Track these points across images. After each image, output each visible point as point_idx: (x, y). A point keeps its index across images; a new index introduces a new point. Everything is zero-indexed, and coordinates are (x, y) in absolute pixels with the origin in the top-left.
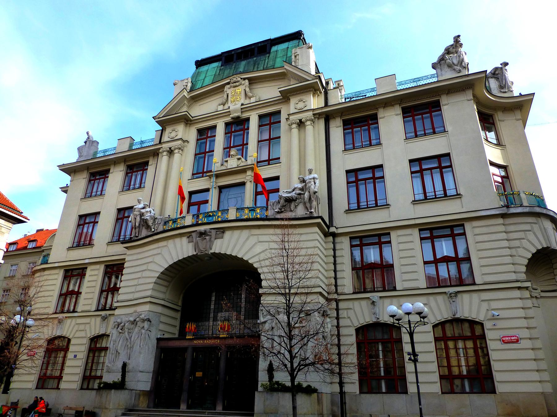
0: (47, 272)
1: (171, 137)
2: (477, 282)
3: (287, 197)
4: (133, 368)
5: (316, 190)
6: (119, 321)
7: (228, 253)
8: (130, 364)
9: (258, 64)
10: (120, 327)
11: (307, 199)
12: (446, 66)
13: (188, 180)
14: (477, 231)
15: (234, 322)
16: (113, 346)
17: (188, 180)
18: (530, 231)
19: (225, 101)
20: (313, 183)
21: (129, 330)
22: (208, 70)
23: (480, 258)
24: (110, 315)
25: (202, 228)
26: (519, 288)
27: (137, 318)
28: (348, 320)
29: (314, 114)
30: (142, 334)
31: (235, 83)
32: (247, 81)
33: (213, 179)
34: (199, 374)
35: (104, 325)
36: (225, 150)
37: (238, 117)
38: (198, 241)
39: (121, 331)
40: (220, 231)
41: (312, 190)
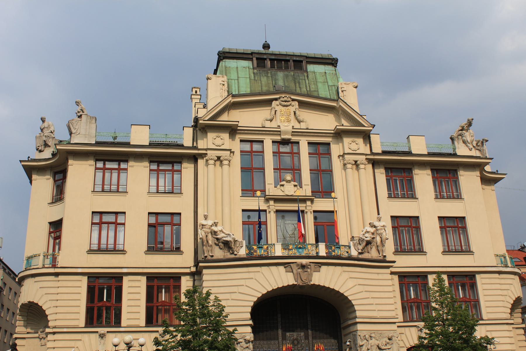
0: (61, 277)
1: (216, 145)
2: (484, 318)
5: (387, 237)
9: (299, 83)
12: (461, 141)
14: (484, 281)
15: (303, 341)
18: (512, 284)
19: (273, 117)
20: (384, 230)
22: (237, 68)
23: (486, 301)
25: (304, 261)
26: (507, 324)
27: (240, 339)
28: (402, 341)
29: (366, 159)
31: (285, 102)
32: (297, 103)
37: (289, 139)
40: (318, 265)
41: (384, 237)
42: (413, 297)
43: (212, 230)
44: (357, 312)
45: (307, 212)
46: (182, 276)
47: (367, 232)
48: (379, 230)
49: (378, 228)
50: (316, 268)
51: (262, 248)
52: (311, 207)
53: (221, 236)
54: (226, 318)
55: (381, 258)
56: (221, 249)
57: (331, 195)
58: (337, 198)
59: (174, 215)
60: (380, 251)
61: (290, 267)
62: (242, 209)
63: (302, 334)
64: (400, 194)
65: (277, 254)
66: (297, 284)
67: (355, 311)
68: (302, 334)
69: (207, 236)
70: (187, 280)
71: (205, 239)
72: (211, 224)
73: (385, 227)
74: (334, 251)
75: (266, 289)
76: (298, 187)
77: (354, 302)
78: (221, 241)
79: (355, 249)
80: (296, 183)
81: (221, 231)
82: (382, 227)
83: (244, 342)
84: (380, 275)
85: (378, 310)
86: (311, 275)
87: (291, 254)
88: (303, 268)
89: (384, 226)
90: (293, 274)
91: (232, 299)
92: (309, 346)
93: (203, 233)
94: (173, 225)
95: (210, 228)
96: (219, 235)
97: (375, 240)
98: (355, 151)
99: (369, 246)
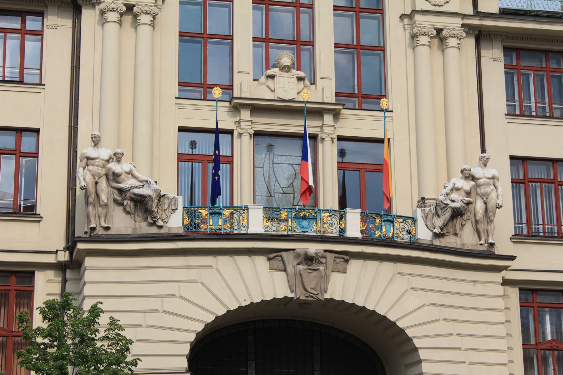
5: (500, 202)
20: (492, 187)
25: (312, 248)
29: (463, 25)
38: (303, 273)
40: (343, 258)
41: (493, 201)
42: (549, 337)
43: (109, 170)
44: (424, 364)
45: (323, 139)
46: (38, 271)
47: (456, 189)
48: (481, 185)
49: (481, 181)
50: (337, 264)
51: (220, 214)
52: (333, 128)
53: (130, 184)
54: (133, 368)
55: (484, 248)
56: (128, 213)
57: (379, 103)
58: (392, 111)
59: (23, 133)
60: (482, 234)
61: (279, 258)
62: (179, 127)
64: (533, 109)
65: (253, 230)
66: (293, 298)
67: (420, 362)
69: (96, 183)
70: (49, 281)
71: (91, 189)
72: (107, 158)
73: (496, 181)
74: (380, 228)
75: (225, 306)
76: (307, 82)
77: (417, 343)
78: (128, 195)
79: (427, 225)
80: (302, 74)
81: (130, 173)
82: (490, 179)
84: (479, 286)
85: (472, 363)
86: (326, 278)
87: (285, 230)
88: (309, 263)
89: (493, 178)
90: (287, 274)
91: (148, 326)
93: (89, 177)
94: (20, 156)
95: (104, 167)
96: (125, 181)
97: (472, 207)
98: (439, 6)
99: (458, 221)
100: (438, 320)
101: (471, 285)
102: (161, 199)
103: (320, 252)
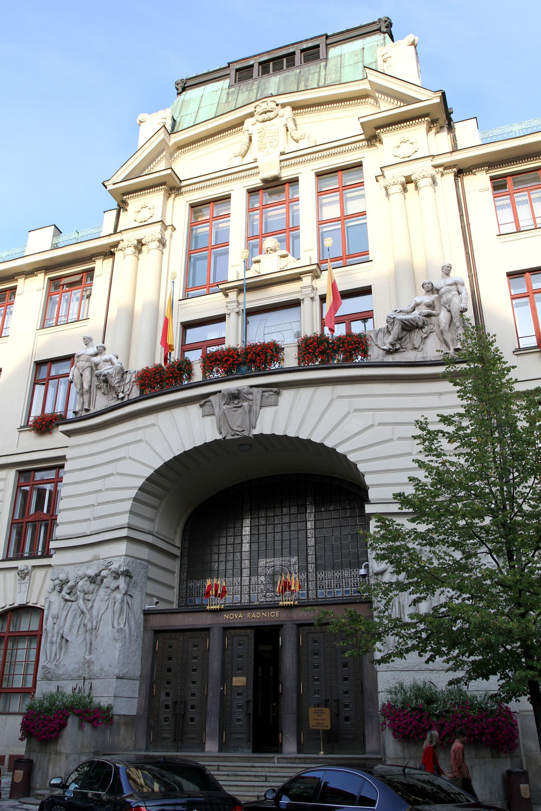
3: (406, 320)
4: (102, 669)
6: (62, 576)
7: (291, 434)
8: (95, 662)
10: (65, 589)
11: (446, 324)
13: (179, 300)
16: (53, 628)
17: (179, 300)
21: (85, 594)
24: (34, 567)
27: (103, 570)
30: (115, 603)
31: (265, 112)
32: (289, 109)
33: (233, 295)
34: (239, 681)
35: (24, 588)
36: (251, 242)
38: (226, 412)
39: (68, 597)
40: (272, 391)
41: (455, 306)
43: (92, 362)
50: (268, 397)
58: (372, 261)
60: (450, 343)
63: (294, 559)
68: (294, 559)
75: (163, 459)
80: (285, 252)
83: (109, 576)
91: (107, 490)
92: (308, 588)
95: (88, 360)
99: (417, 337)
100: (391, 440)
101: (436, 397)
102: (125, 376)
103: (244, 389)
